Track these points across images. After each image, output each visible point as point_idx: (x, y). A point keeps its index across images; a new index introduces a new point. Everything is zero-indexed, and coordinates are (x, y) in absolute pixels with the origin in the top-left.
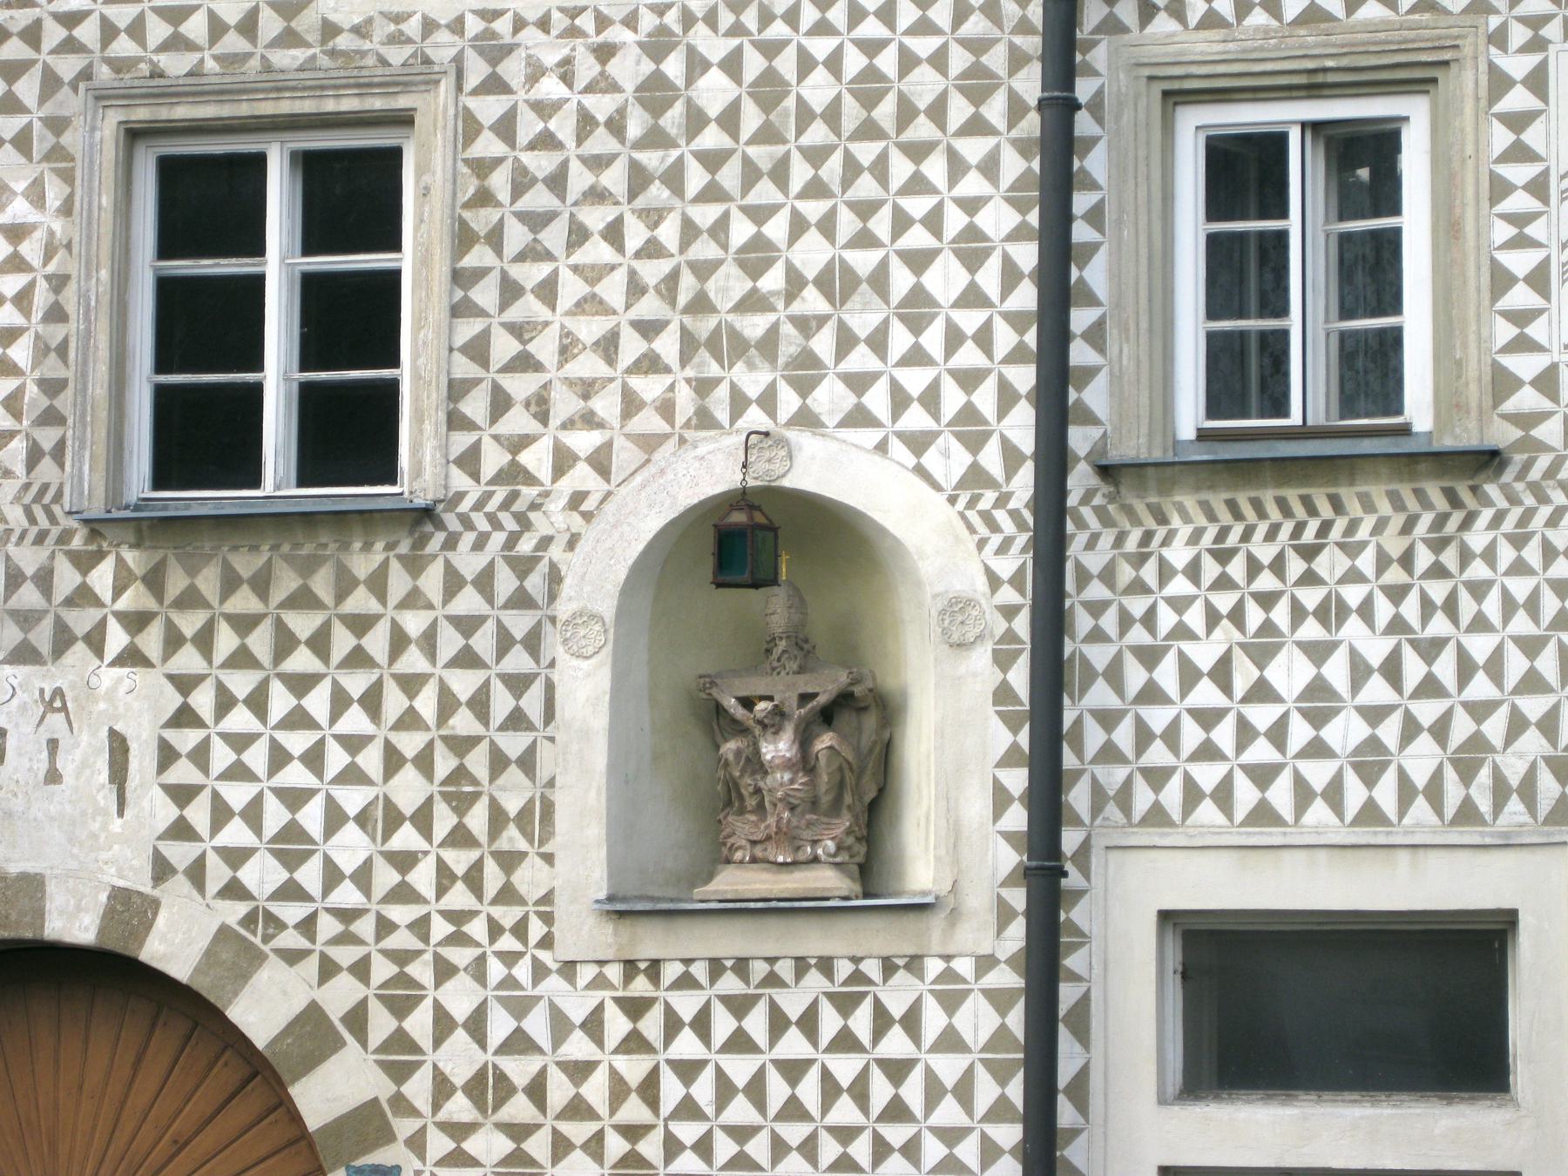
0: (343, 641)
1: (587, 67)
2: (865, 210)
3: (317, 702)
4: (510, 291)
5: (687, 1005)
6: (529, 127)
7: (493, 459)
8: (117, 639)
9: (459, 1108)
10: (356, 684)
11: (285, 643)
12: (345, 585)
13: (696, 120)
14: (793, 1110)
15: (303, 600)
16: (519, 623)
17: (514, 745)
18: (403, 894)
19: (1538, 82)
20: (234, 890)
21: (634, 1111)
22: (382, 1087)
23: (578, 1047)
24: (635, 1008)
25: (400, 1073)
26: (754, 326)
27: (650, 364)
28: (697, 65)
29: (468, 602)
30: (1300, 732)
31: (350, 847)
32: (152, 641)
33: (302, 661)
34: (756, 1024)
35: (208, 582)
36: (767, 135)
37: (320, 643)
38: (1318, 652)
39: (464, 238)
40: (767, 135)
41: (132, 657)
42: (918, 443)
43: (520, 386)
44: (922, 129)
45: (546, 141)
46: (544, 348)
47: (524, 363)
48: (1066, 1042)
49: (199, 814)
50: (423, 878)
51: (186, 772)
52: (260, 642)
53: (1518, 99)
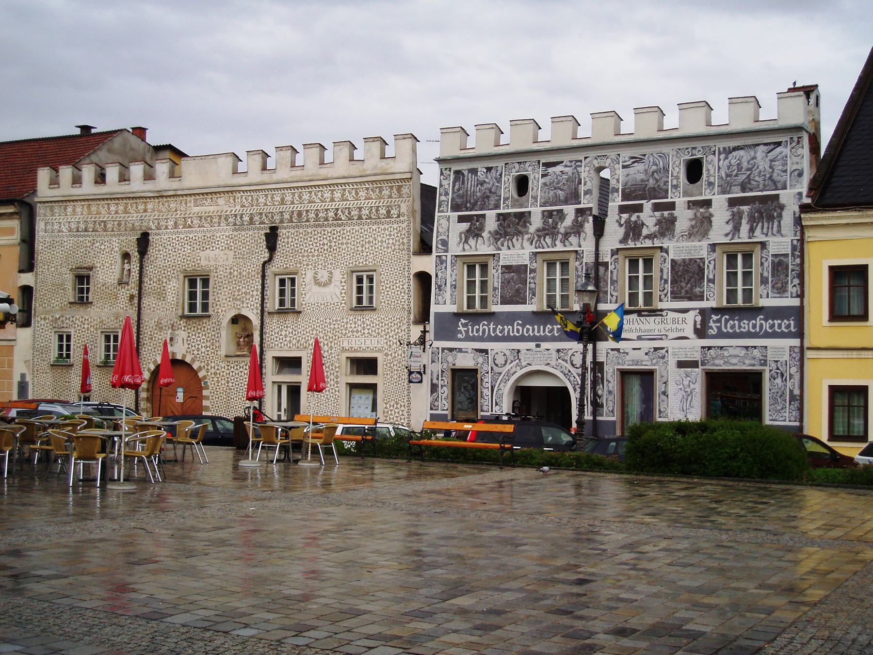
0: (203, 329)
1: (225, 271)
2: (248, 286)
3: (200, 335)
4: (218, 293)
5: (232, 366)
6: (219, 277)
7: (216, 311)
8: (183, 328)
9: (213, 376)
10: (204, 333)
11: (198, 329)
12: (203, 323)
13: (234, 276)
14: (241, 376)
15: (199, 325)
16: (218, 327)
17: (217, 339)
18: (208, 354)
19: (305, 274)
20: (193, 354)
21: (228, 376)
22: (206, 374)
23: (223, 370)
24: (228, 366)
25: (208, 372)
26: (239, 297)
27: (230, 301)
28: (234, 271)
29: (214, 325)
30: (284, 339)
31: (203, 350)
32: (186, 329)
33: (199, 331)
34: (238, 367)
35: (191, 323)
36: (240, 278)
37: (201, 329)
38: (286, 331)
39: (214, 288)
40: (240, 278)
41: (184, 330)
42: (252, 310)
43: (218, 303)
44: (253, 278)
45: (221, 278)
46: (220, 300)
47: (219, 301)
48: (264, 369)
49: (190, 346)
50: (210, 353)
51: (189, 342)
52: (196, 329)
53: (304, 276)
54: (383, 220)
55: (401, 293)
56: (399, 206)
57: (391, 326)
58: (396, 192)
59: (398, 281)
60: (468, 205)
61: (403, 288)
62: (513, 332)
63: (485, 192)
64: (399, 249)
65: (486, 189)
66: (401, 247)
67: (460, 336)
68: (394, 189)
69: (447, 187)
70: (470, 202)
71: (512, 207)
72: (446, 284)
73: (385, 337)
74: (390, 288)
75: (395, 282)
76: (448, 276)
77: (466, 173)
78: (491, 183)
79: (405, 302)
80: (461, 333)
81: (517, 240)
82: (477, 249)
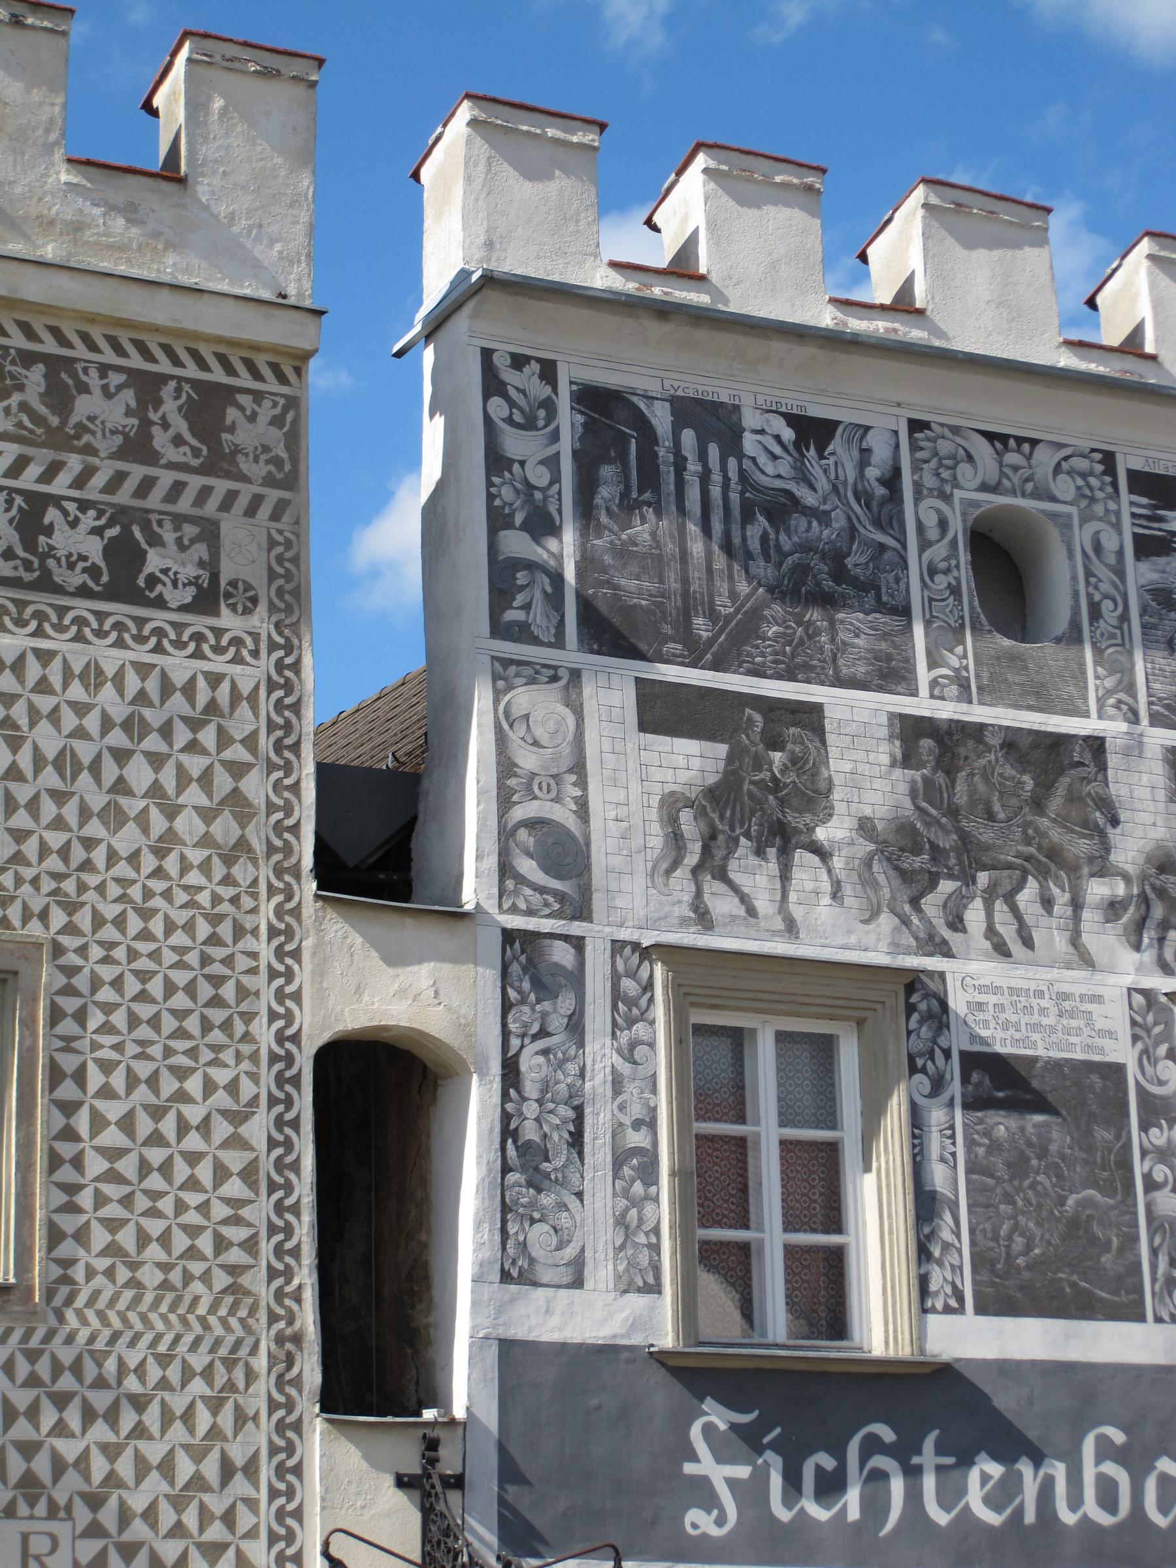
54: (82, 607)
55: (221, 1173)
56: (210, 533)
57: (140, 1431)
58: (180, 425)
59: (194, 1085)
60: (701, 626)
61: (236, 1142)
62: (1075, 1502)
63: (802, 570)
64: (205, 841)
65: (806, 547)
66: (225, 828)
67: (698, 1521)
68: (170, 406)
69: (539, 476)
70: (712, 615)
71: (991, 692)
72: (577, 1140)
73: (82, 1515)
74: (127, 1124)
75: (169, 1085)
76: (597, 1083)
77: (661, 418)
78: (839, 521)
79: (250, 1246)
80: (710, 1502)
81: (1047, 903)
82: (791, 928)
